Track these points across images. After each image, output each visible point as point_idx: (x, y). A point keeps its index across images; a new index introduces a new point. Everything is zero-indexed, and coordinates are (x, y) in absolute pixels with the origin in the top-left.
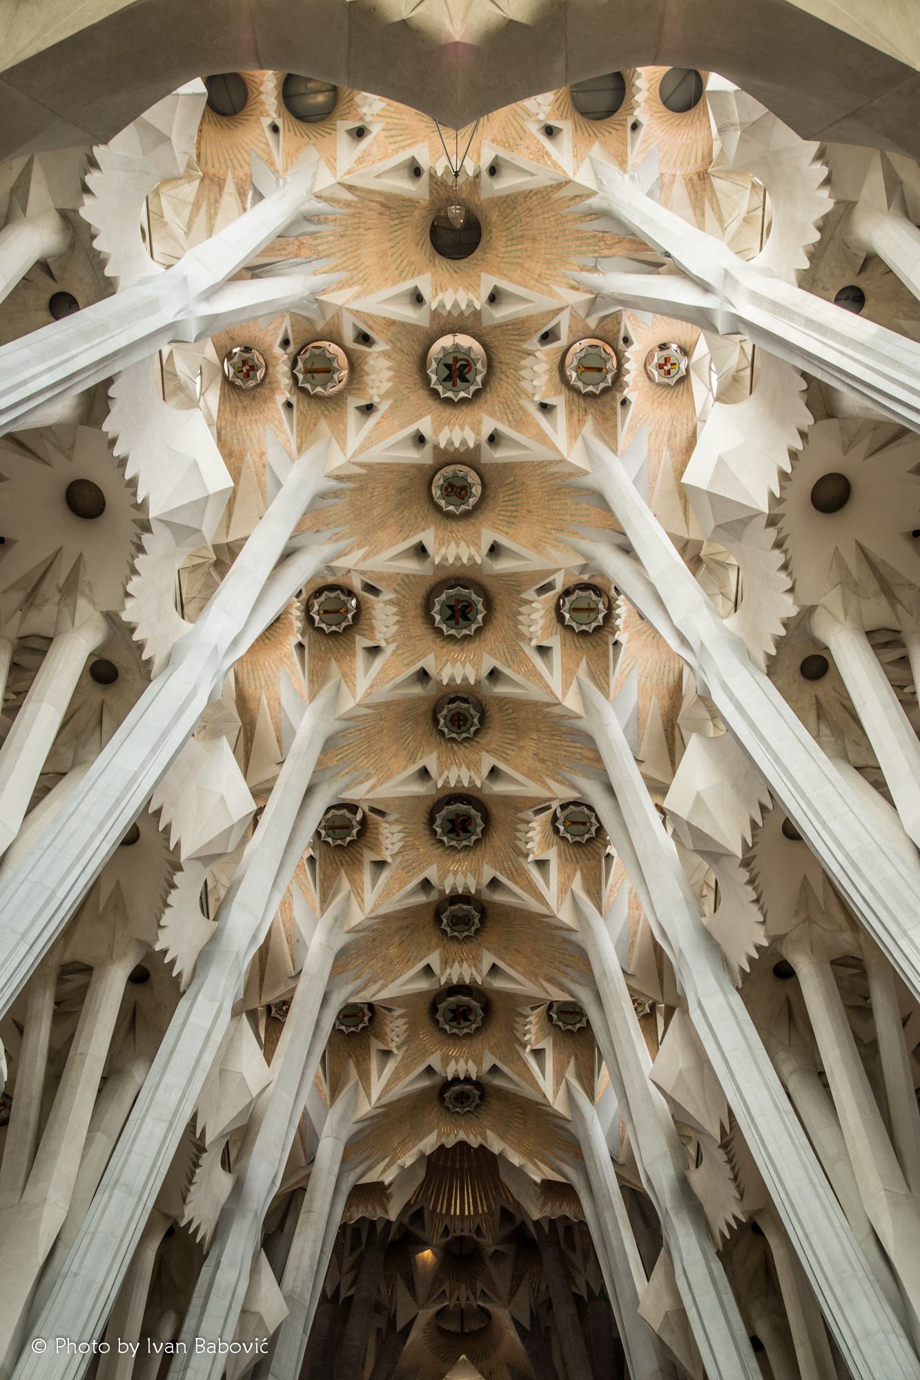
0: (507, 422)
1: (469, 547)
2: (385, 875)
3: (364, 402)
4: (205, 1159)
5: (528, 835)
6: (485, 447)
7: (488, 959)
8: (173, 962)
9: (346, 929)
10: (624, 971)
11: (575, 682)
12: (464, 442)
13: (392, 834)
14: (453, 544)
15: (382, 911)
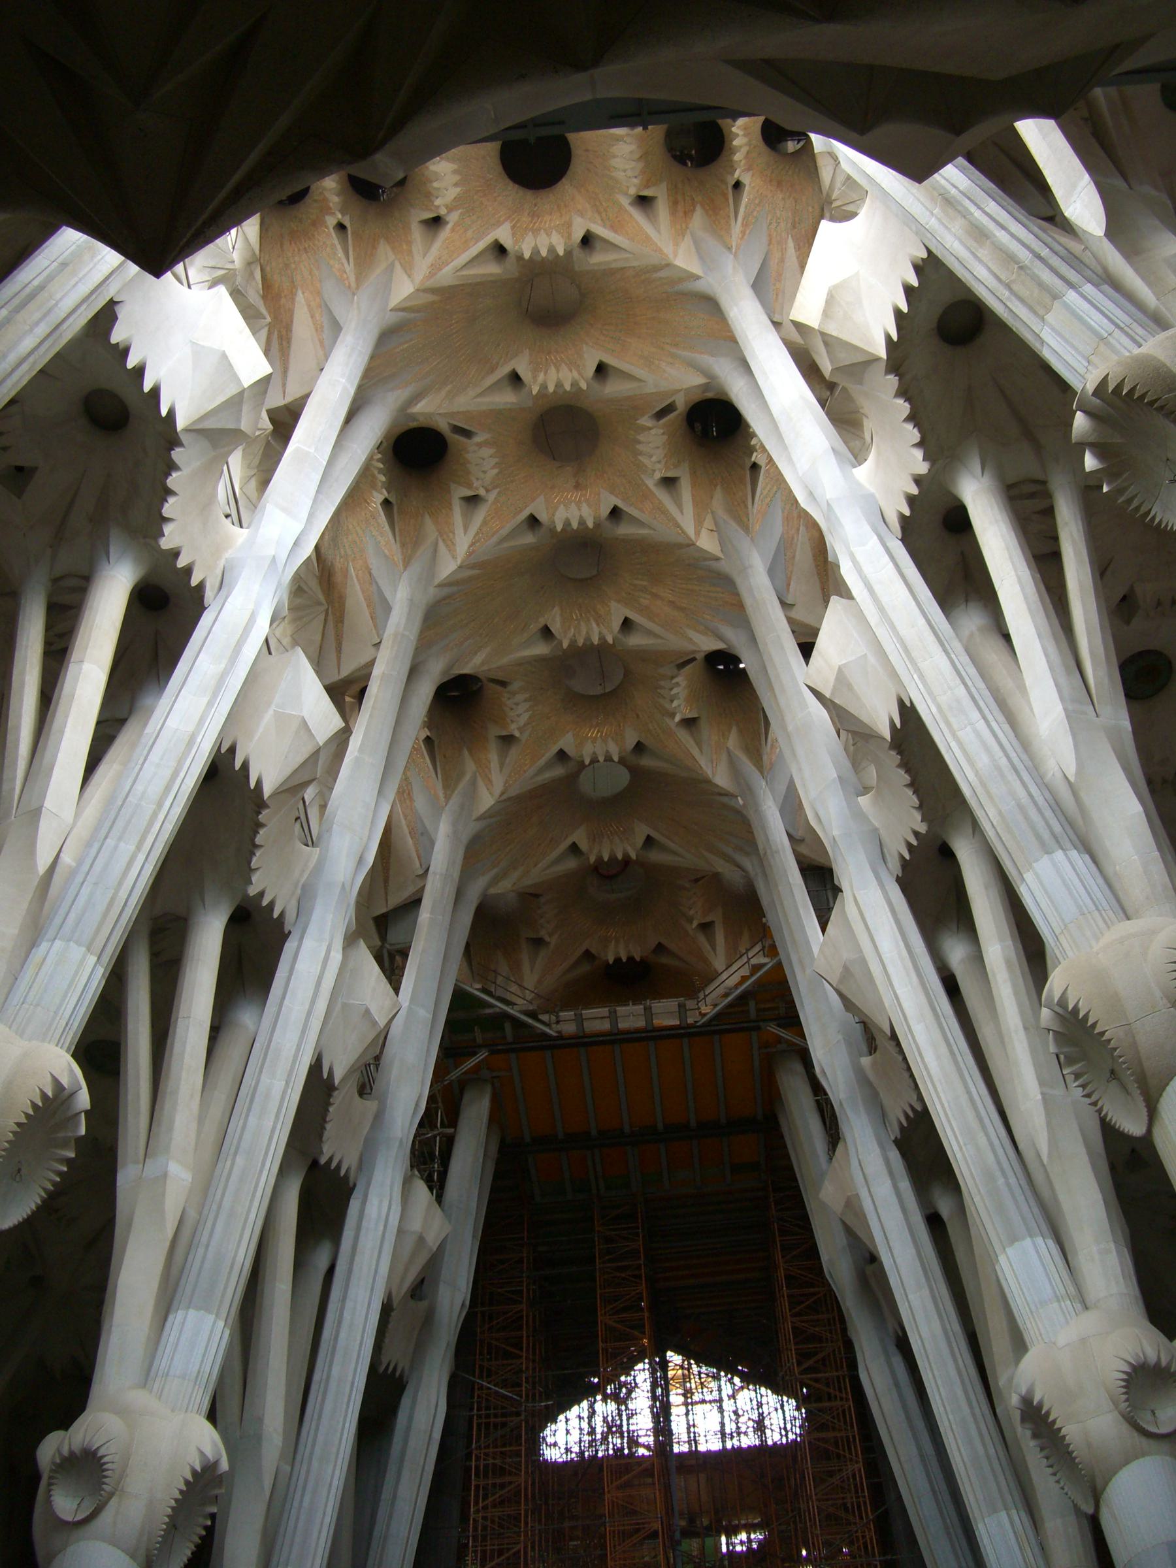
0: (600, 222)
1: (571, 371)
2: (514, 752)
3: (430, 215)
4: (337, 1098)
5: (673, 692)
6: (578, 253)
7: (641, 831)
8: (271, 905)
9: (474, 818)
10: (790, 836)
11: (709, 518)
12: (552, 250)
13: (517, 704)
14: (553, 370)
15: (513, 792)
